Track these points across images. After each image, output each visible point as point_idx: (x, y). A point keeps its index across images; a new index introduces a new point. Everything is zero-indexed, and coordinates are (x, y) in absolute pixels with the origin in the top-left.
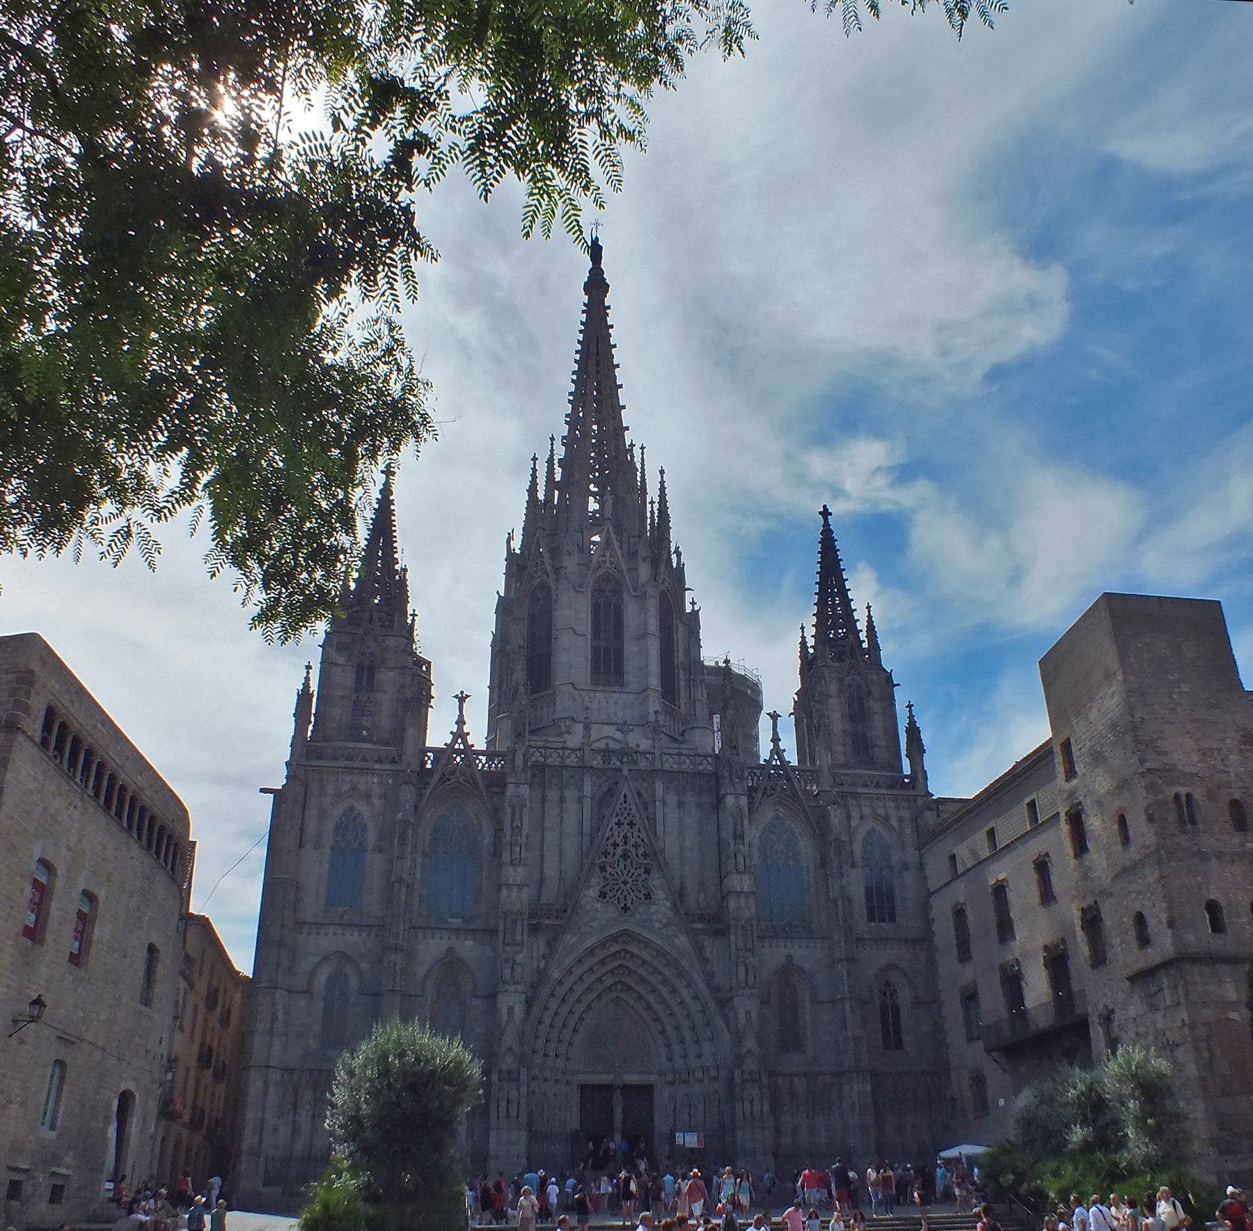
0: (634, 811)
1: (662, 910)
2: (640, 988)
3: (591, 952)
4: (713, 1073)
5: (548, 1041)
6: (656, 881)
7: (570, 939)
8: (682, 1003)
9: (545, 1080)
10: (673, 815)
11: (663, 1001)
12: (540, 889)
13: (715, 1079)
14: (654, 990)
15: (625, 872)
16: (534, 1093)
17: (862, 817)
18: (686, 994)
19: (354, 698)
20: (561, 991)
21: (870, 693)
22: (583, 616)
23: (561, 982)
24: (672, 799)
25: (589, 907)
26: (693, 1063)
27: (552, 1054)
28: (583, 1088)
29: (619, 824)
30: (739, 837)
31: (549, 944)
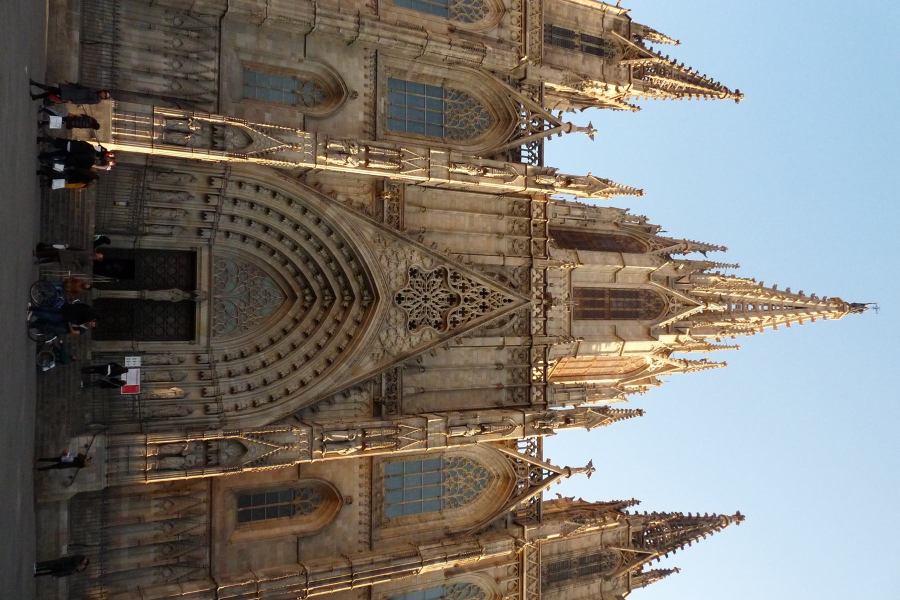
0: (497, 310)
1: (399, 341)
2: (307, 323)
3: (353, 256)
4: (214, 407)
5: (252, 205)
6: (428, 334)
7: (369, 231)
8: (295, 368)
9: (206, 198)
10: (488, 357)
11: (294, 347)
12: (416, 205)
13: (206, 409)
14: (306, 336)
15: (436, 300)
16: (193, 179)
17: (497, 580)
18: (306, 373)
19: (577, 32)
20: (308, 222)
21: (607, 579)
22: (630, 280)
23: (318, 221)
24: (503, 357)
25: (401, 255)
26: (224, 385)
27: (236, 211)
28: (191, 256)
29: (484, 294)
30: (482, 427)
31: (362, 207)
